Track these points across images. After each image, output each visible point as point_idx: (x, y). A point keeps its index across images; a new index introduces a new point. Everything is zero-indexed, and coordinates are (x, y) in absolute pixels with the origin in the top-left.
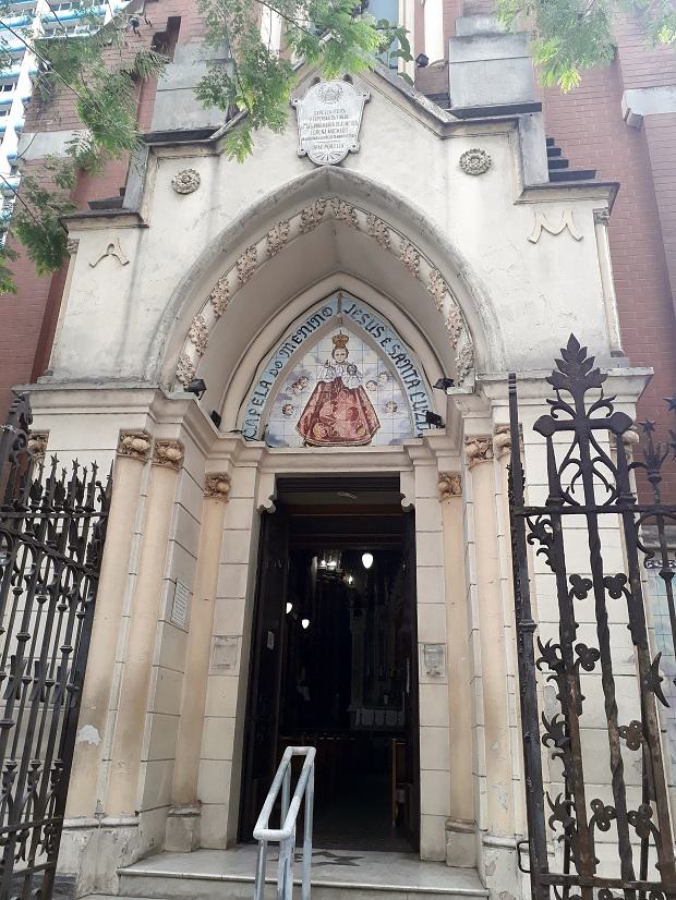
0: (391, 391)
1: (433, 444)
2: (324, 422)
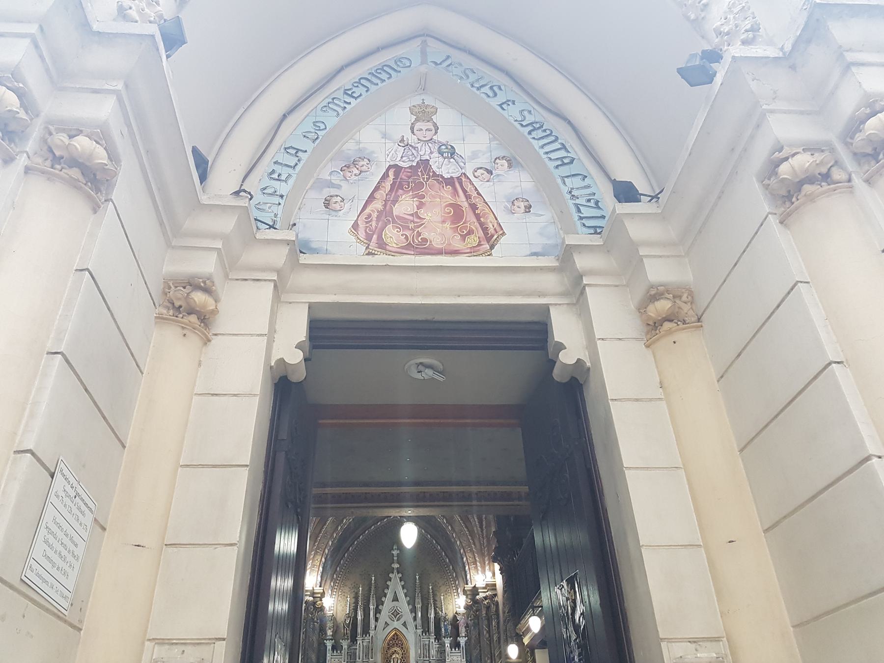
0: (518, 182)
1: (636, 231)
2: (402, 223)
